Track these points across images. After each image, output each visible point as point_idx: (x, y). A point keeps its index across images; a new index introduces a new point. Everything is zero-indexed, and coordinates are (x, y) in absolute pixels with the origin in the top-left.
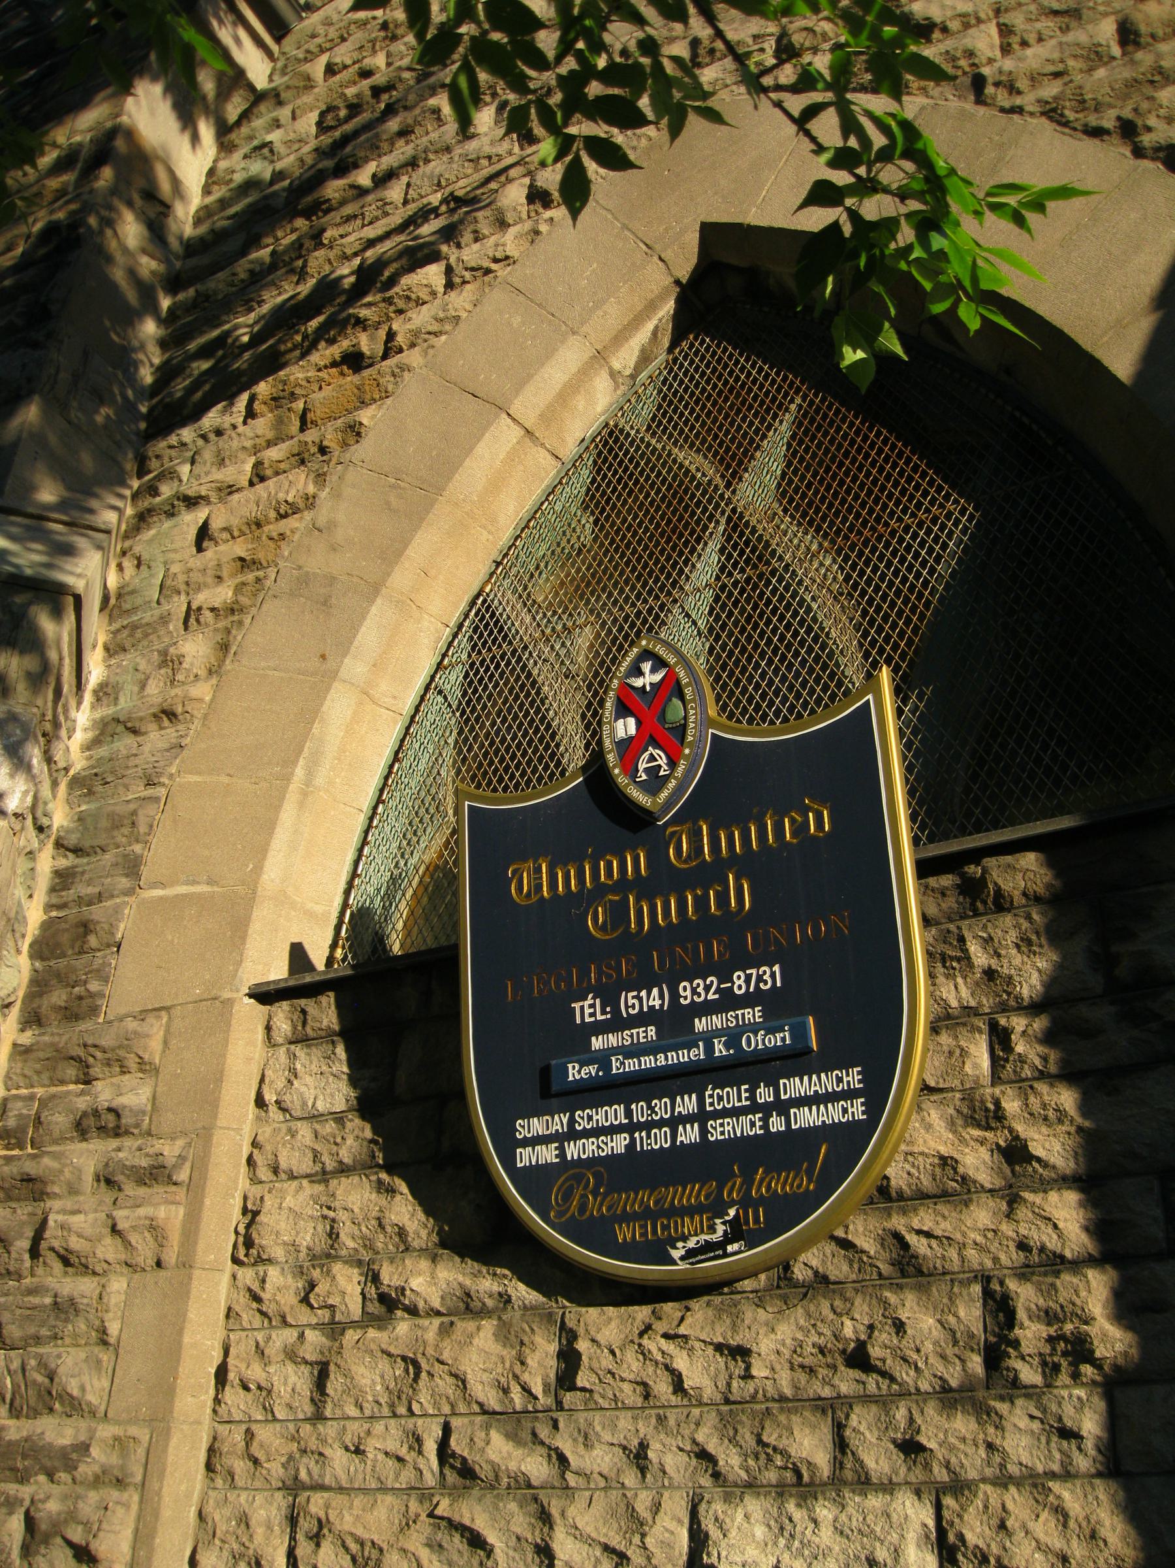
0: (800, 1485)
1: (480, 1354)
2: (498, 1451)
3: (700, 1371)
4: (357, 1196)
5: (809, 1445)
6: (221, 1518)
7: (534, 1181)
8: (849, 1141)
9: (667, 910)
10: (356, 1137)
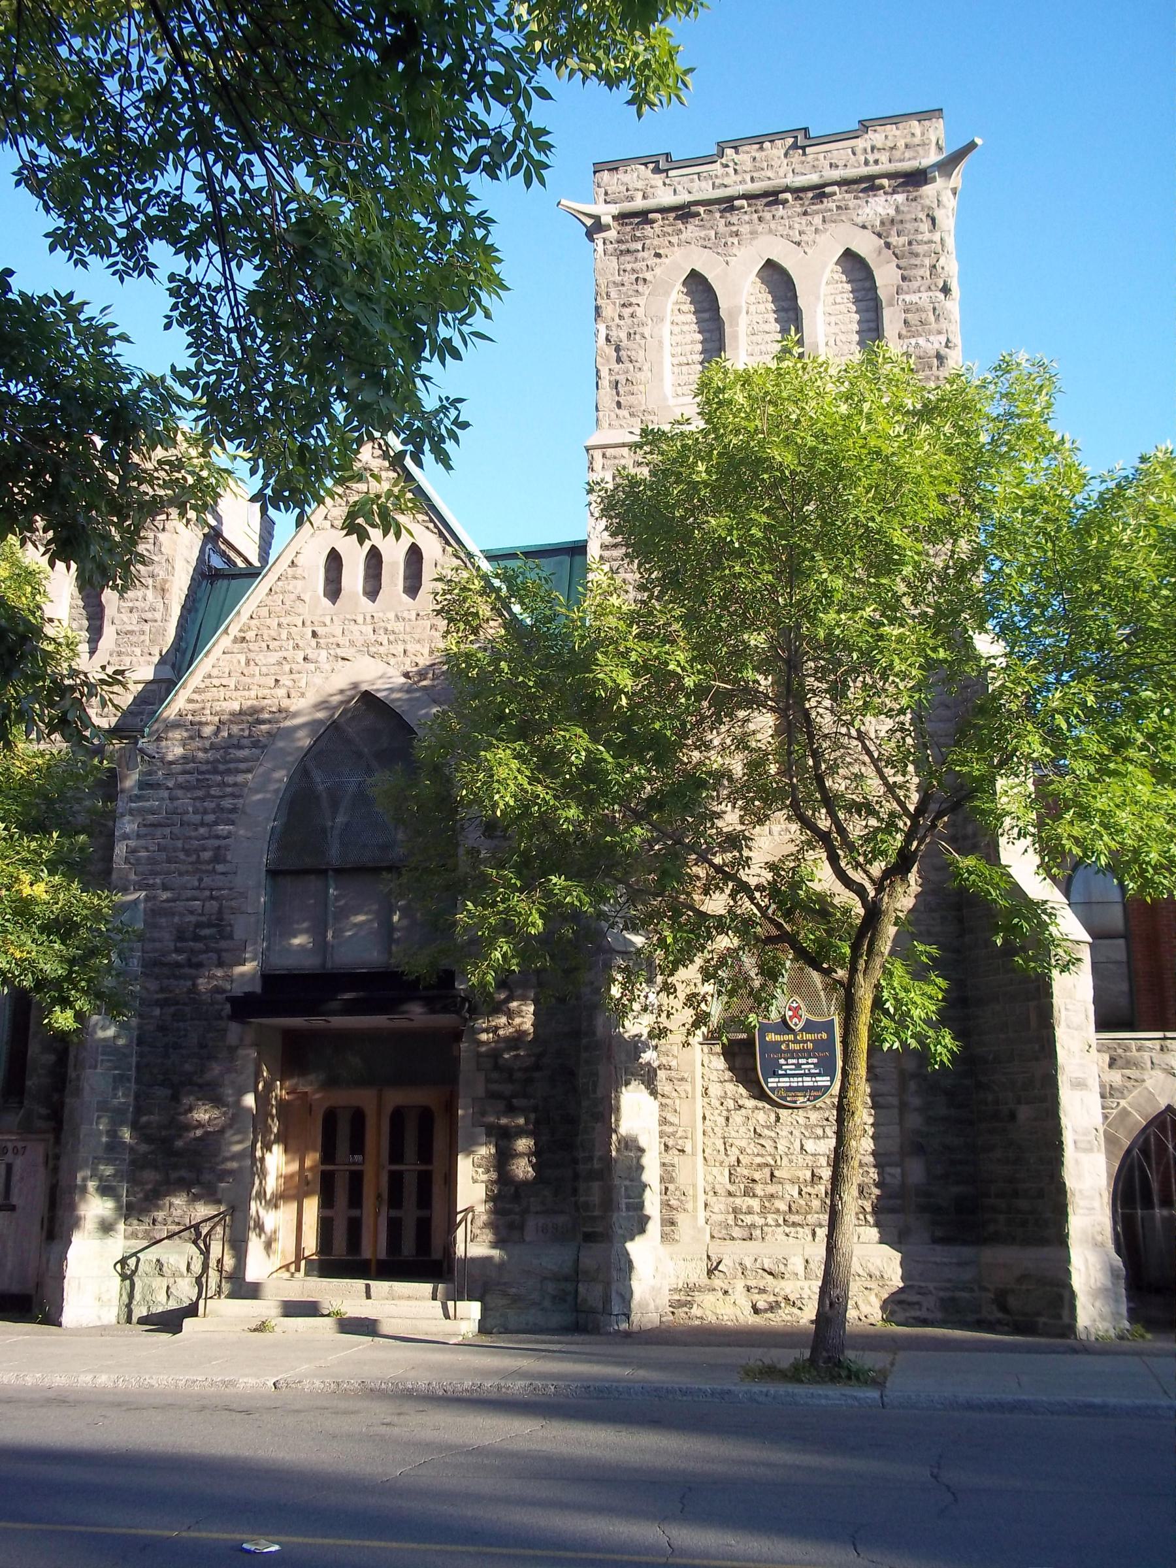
0: (818, 1138)
1: (761, 1116)
2: (766, 1132)
3: (802, 1121)
4: (730, 1087)
5: (820, 1132)
6: (708, 1143)
7: (772, 1089)
8: (828, 1088)
9: (797, 1047)
10: (728, 1075)
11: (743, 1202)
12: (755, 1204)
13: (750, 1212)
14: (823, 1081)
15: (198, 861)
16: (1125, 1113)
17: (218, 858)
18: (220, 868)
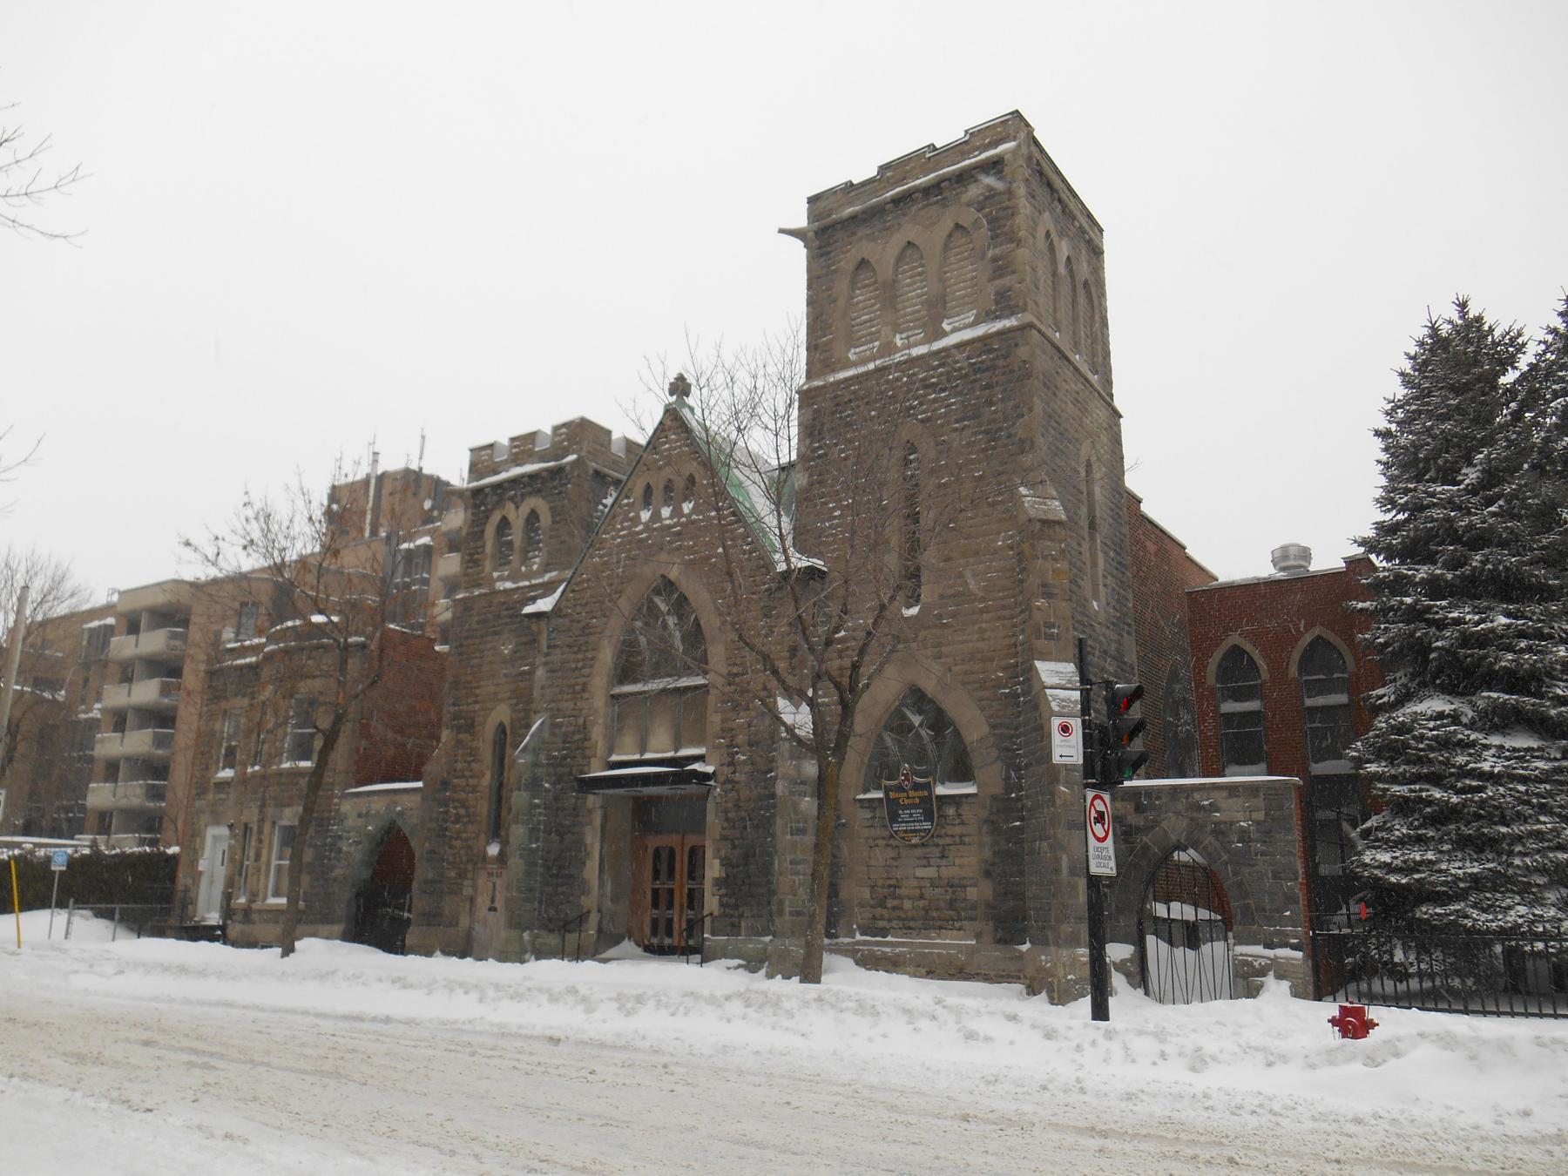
11: (879, 911)
12: (885, 912)
13: (882, 918)
14: (927, 825)
15: (575, 692)
16: (1146, 848)
17: (584, 690)
18: (586, 695)
